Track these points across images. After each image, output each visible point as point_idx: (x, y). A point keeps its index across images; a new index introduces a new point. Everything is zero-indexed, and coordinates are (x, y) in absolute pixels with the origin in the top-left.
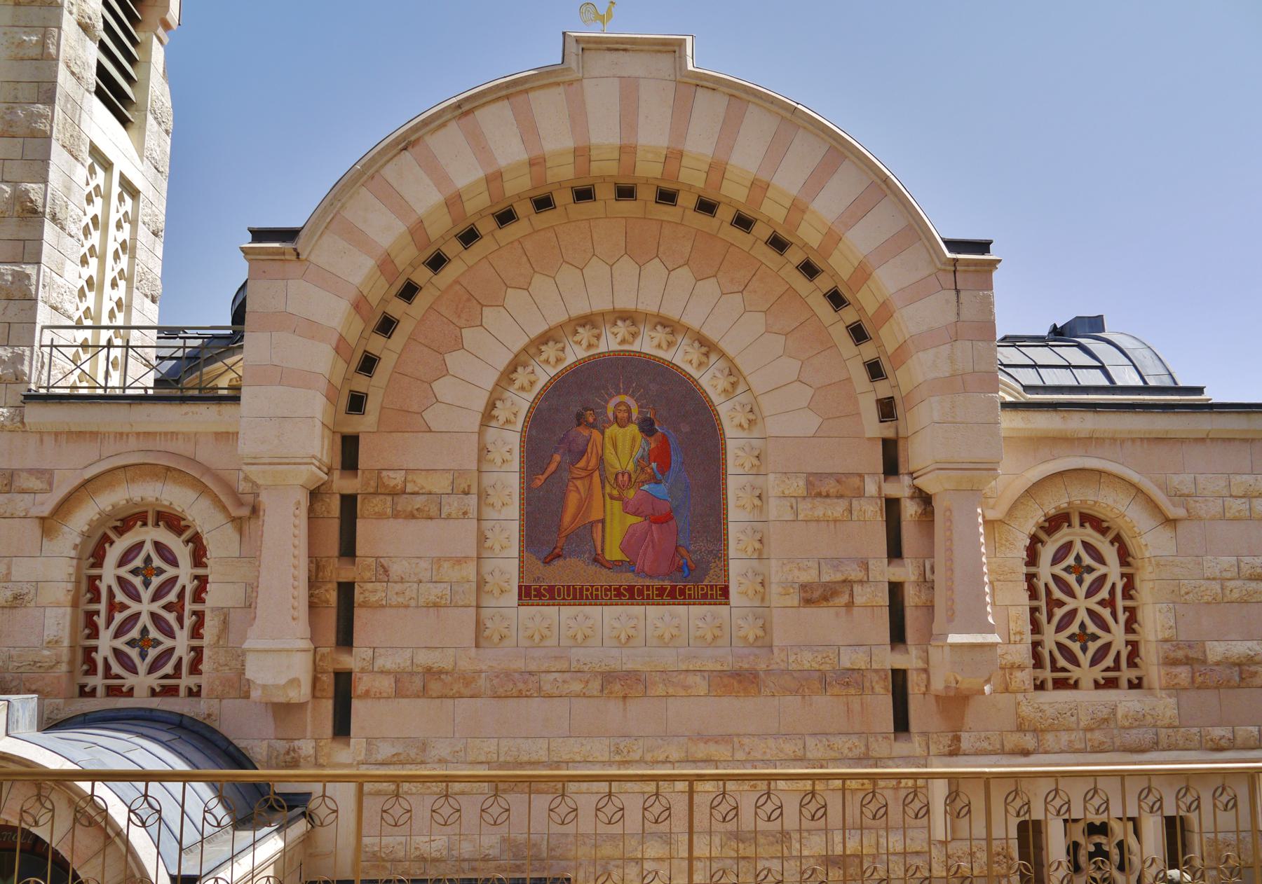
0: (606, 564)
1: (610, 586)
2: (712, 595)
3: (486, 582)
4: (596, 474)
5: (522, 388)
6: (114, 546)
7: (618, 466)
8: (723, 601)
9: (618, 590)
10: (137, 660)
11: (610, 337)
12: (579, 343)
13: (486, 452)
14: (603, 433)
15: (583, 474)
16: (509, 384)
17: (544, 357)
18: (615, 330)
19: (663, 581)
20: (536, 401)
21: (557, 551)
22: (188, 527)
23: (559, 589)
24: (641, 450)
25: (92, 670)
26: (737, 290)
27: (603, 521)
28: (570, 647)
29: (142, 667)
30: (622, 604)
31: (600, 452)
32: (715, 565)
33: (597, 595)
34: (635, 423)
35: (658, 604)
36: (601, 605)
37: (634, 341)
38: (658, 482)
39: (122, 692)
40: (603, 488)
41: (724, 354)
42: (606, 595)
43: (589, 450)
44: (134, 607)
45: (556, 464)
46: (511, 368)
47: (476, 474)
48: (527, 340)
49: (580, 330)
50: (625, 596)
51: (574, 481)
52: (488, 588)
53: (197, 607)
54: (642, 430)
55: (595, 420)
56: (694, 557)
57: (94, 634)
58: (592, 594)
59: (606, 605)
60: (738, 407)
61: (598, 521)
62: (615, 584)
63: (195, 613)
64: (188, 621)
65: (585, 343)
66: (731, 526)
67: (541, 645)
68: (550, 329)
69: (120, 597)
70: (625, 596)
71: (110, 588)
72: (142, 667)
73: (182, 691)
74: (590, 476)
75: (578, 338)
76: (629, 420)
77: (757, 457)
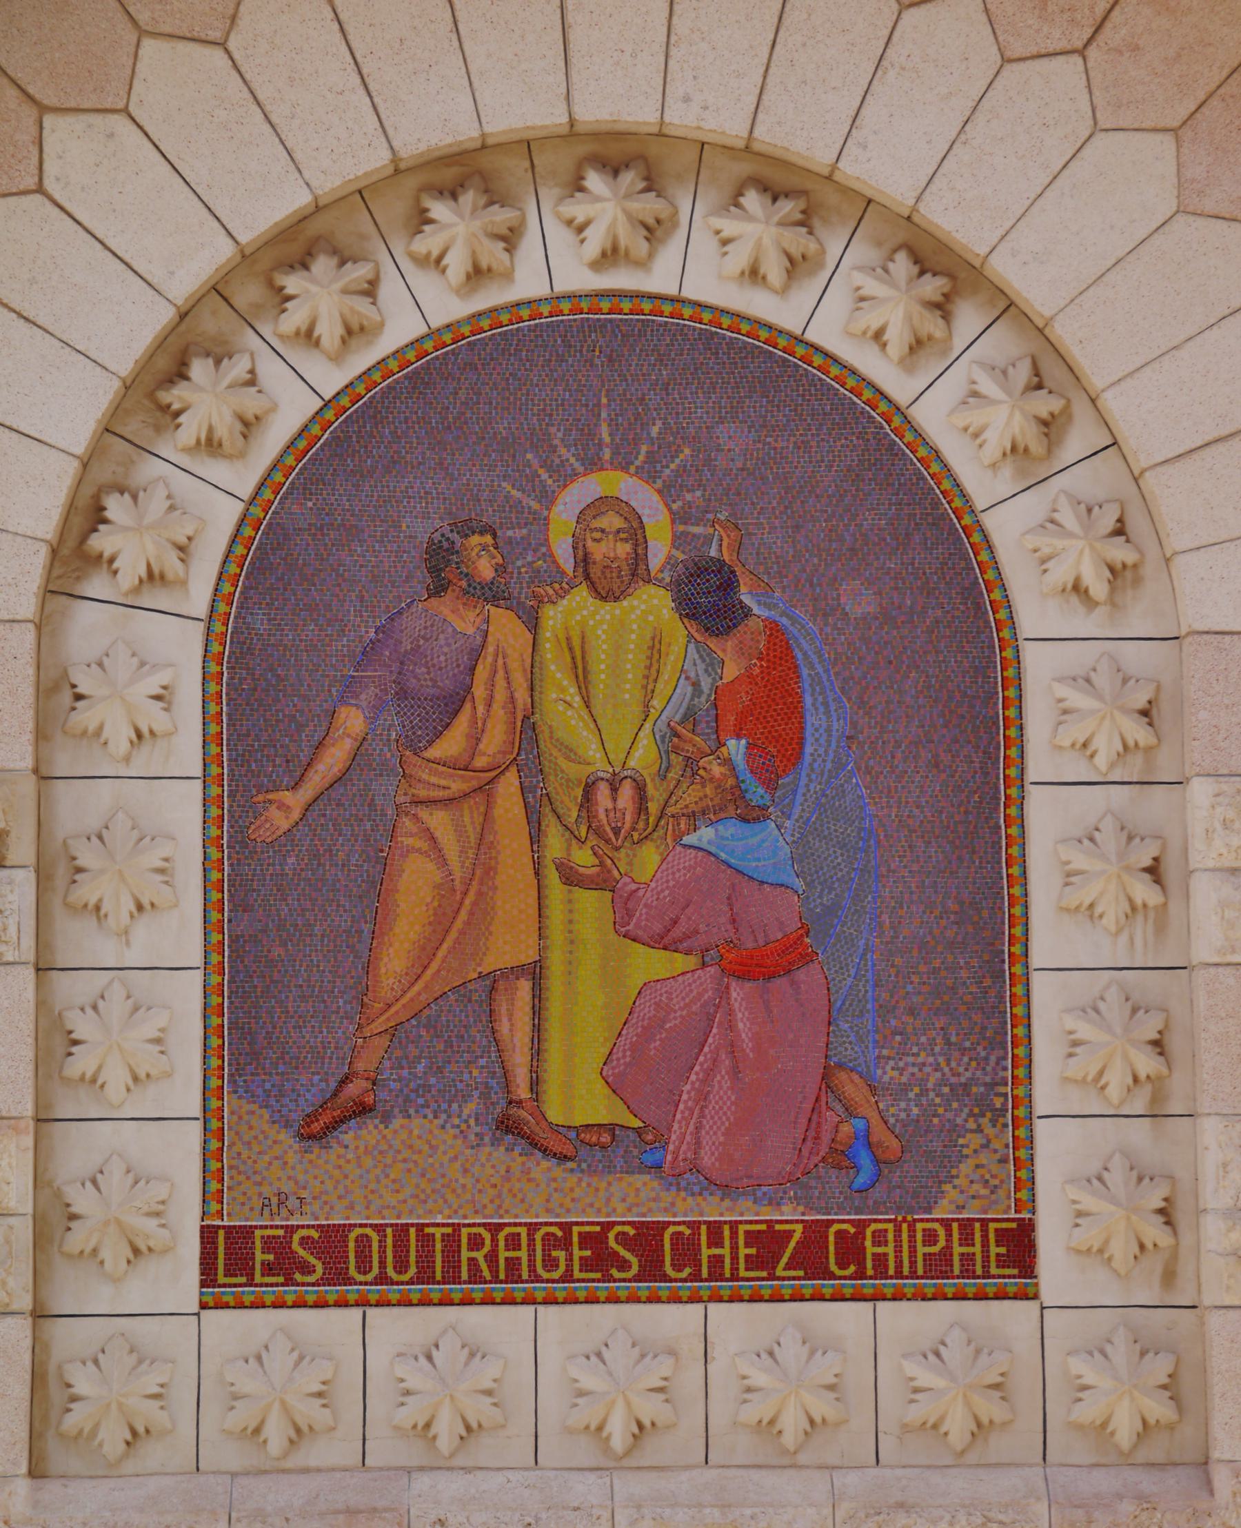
0: (542, 1135)
1: (566, 1227)
2: (967, 1259)
3: (73, 1217)
4: (509, 785)
5: (210, 445)
7: (593, 752)
8: (1012, 1284)
9: (596, 1241)
11: (559, 236)
12: (437, 263)
13: (66, 697)
14: (533, 624)
15: (457, 786)
16: (158, 429)
17: (295, 318)
18: (578, 210)
19: (775, 1203)
20: (267, 494)
21: (353, 1089)
23: (363, 1241)
24: (685, 689)
26: (1063, 45)
27: (536, 972)
28: (409, 1471)
30: (613, 1299)
31: (522, 696)
32: (976, 1140)
33: (513, 1264)
34: (659, 583)
35: (756, 1298)
36: (529, 1300)
37: (651, 255)
38: (752, 816)
40: (536, 838)
41: (1012, 304)
42: (551, 1264)
43: (479, 691)
45: (347, 745)
46: (164, 363)
47: (28, 786)
48: (224, 251)
49: (439, 210)
50: (624, 1265)
51: (423, 813)
52: (78, 1239)
54: (688, 609)
55: (500, 569)
56: (895, 1112)
58: (492, 1258)
59: (550, 1301)
60: (1068, 518)
61: (518, 971)
62: (586, 1216)
65: (457, 263)
66: (1042, 987)
67: (289, 1464)
68: (318, 208)
70: (624, 1265)
74: (485, 790)
75: (428, 242)
76: (637, 570)
77: (1145, 713)
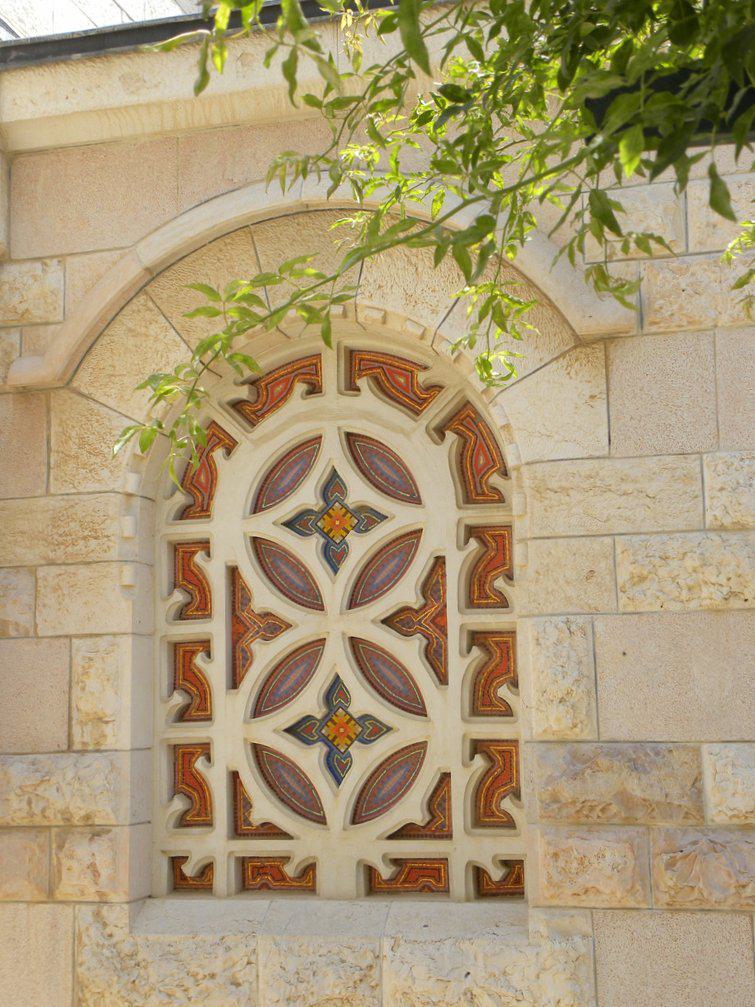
6: (238, 453)
10: (321, 781)
22: (435, 388)
25: (196, 816)
29: (337, 801)
39: (283, 878)
44: (303, 625)
53: (487, 620)
57: (197, 708)
63: (476, 638)
64: (461, 664)
69: (264, 597)
71: (233, 573)
72: (337, 801)
73: (459, 880)
